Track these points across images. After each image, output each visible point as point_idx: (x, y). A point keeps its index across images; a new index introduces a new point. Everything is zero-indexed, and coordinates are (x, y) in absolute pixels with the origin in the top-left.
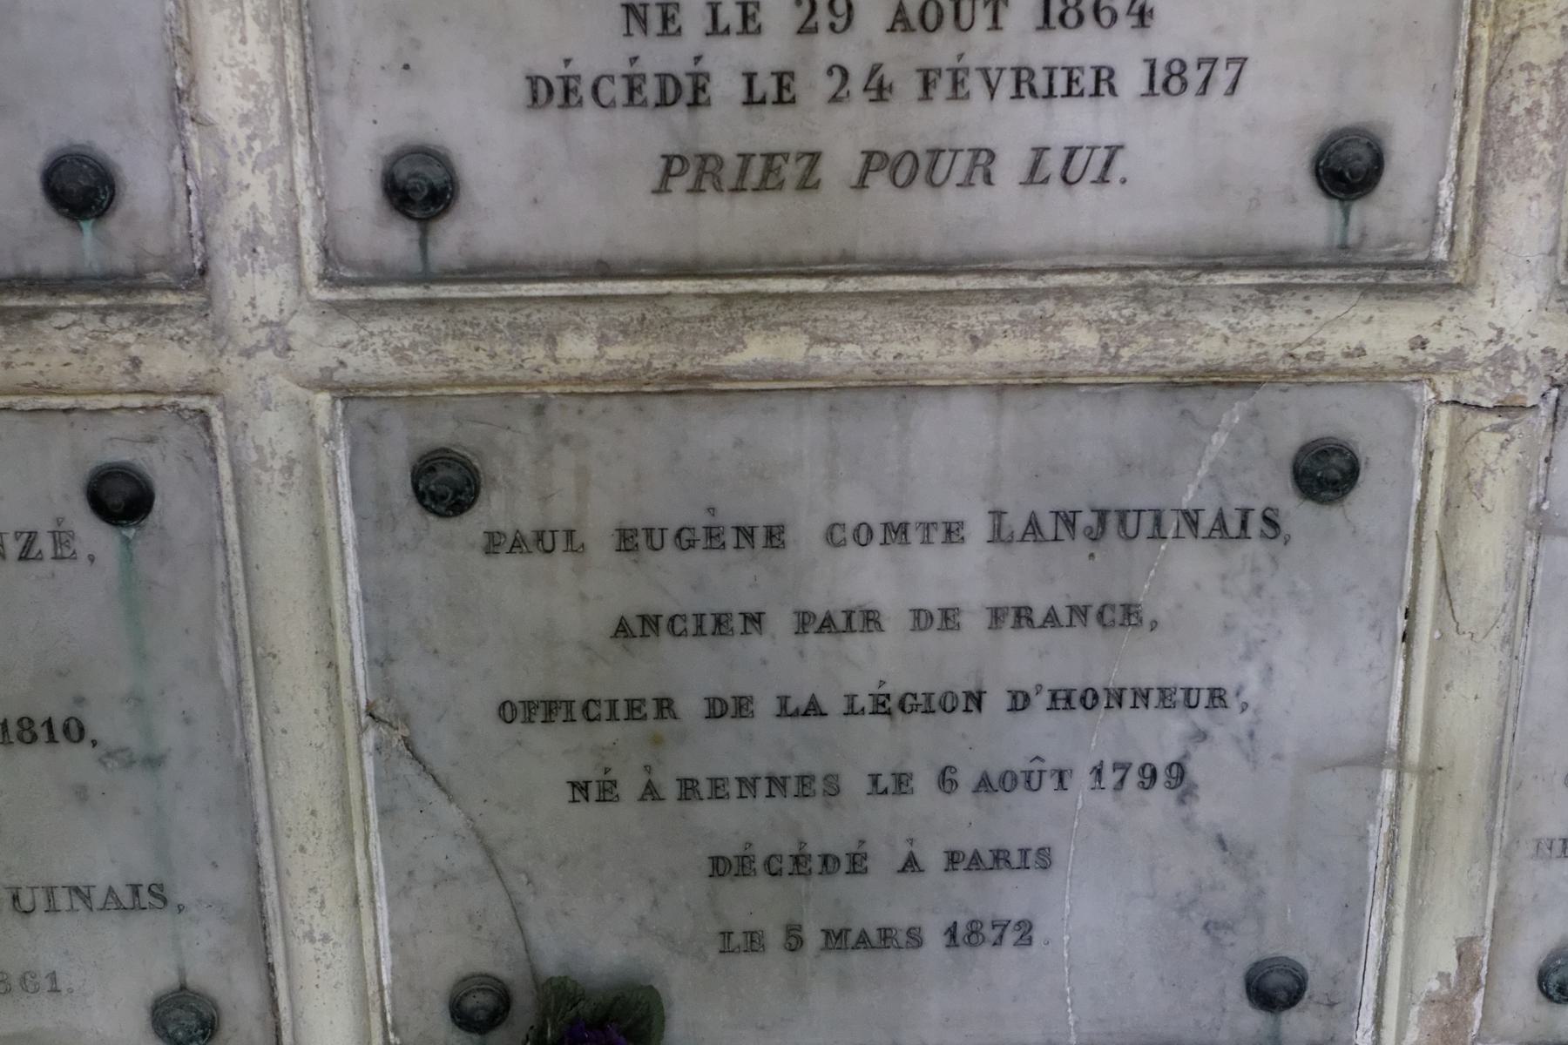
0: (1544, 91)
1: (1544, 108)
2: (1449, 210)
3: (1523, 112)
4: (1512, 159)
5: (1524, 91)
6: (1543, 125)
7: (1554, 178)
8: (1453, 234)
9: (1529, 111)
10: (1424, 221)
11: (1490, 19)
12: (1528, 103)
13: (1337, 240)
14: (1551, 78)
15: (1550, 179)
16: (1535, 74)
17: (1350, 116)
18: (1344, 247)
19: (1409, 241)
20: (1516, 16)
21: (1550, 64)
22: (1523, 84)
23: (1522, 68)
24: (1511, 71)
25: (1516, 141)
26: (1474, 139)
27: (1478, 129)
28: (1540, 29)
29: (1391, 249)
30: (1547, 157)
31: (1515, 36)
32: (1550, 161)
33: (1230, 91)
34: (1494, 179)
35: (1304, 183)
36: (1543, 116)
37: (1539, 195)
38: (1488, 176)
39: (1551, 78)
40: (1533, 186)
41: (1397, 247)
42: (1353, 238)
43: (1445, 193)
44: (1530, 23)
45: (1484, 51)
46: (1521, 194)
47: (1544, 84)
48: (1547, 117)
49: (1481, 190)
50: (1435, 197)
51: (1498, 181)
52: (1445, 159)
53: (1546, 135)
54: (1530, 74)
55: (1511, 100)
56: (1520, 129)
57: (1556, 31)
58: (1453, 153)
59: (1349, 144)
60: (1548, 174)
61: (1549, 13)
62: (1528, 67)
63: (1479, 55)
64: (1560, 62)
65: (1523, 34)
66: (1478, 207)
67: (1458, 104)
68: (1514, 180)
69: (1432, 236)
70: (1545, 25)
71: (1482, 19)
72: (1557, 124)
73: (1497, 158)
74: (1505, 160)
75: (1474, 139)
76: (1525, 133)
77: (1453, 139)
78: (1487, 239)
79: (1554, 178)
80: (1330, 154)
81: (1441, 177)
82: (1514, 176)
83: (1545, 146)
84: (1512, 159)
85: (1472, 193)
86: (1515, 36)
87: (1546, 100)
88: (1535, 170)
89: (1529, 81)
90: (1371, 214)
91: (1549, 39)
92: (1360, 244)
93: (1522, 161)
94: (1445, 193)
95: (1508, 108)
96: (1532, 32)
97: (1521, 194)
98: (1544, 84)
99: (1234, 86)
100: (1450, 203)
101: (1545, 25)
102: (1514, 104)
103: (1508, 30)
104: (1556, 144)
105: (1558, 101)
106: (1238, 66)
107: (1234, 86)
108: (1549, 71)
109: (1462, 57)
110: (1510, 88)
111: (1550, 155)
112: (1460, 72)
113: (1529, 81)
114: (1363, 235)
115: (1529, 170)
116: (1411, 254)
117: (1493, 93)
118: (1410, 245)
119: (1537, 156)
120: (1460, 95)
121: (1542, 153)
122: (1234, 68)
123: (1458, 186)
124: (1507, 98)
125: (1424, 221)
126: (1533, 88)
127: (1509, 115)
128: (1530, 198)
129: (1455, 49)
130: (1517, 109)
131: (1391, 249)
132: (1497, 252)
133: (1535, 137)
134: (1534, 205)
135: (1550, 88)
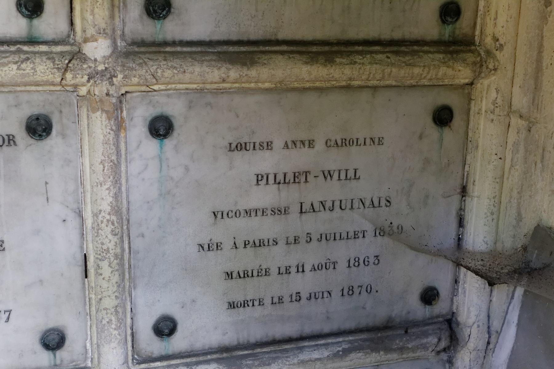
0: (112, 316)
1: (113, 321)
2: (90, 350)
3: (106, 323)
4: (105, 337)
5: (106, 316)
6: (113, 326)
7: (120, 341)
8: (92, 359)
9: (108, 322)
10: (82, 354)
11: (94, 292)
12: (108, 320)
13: (53, 363)
14: (114, 312)
15: (119, 341)
16: (108, 311)
17: (51, 325)
18: (56, 365)
19: (78, 361)
20: (100, 293)
21: (113, 308)
22: (105, 314)
23: (104, 309)
24: (101, 310)
25: (105, 331)
26: (94, 328)
27: (95, 326)
28: (108, 297)
29: (72, 364)
30: (117, 335)
31: (101, 299)
32: (118, 337)
33: (7, 320)
34: (101, 343)
35: (39, 347)
36: (113, 324)
37: (116, 348)
38: (99, 341)
39: (114, 312)
40: (113, 345)
41: (74, 363)
42: (58, 362)
43: (88, 345)
44: (105, 295)
45: (93, 302)
46: (110, 348)
47: (112, 314)
48: (115, 324)
49: (98, 346)
50: (85, 347)
51: (102, 344)
52: (87, 335)
53: (115, 329)
54: (106, 311)
55: (102, 319)
56: (106, 328)
57: (114, 298)
58: (89, 333)
59: (51, 335)
60: (118, 341)
61: (110, 292)
62: (106, 309)
63: (92, 303)
64: (117, 306)
65: (103, 299)
66: (98, 351)
67: (88, 317)
68: (106, 344)
69: (86, 359)
70: (109, 296)
71: (92, 292)
72: (119, 325)
73: (101, 336)
74: (103, 337)
75: (94, 328)
76: (108, 329)
77: (89, 327)
78: (101, 361)
79: (120, 341)
80: (45, 338)
81: (86, 340)
82: (106, 342)
83: (116, 332)
84: (105, 337)
85: (96, 346)
86: (101, 299)
87: (113, 318)
88: (113, 340)
89: (107, 314)
90: (63, 354)
91: (111, 300)
92: (61, 364)
93: (108, 338)
94: (88, 345)
95: (102, 321)
96: (105, 298)
97: (110, 348)
98: (112, 314)
99: (8, 318)
100: (90, 348)
101: (109, 296)
102: (103, 320)
103: (99, 297)
104: (119, 331)
105: (118, 318)
106: (9, 313)
107: (8, 318)
108: (113, 310)
109: (88, 303)
110: (102, 315)
111: (118, 334)
112: (88, 307)
113: (107, 314)
114: (62, 361)
115: (111, 340)
116: (80, 365)
117: (97, 315)
118: (79, 362)
119: (113, 336)
120: (88, 315)
121: (115, 335)
122: (7, 314)
123: (91, 344)
124: (101, 318)
125: (82, 354)
126: (108, 315)
127: (102, 323)
128: (113, 349)
129: (85, 300)
130: (104, 322)
131: (72, 364)
132: (105, 366)
133: (111, 330)
134: (115, 351)
135: (114, 315)
